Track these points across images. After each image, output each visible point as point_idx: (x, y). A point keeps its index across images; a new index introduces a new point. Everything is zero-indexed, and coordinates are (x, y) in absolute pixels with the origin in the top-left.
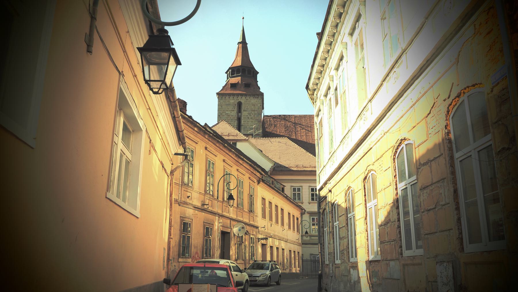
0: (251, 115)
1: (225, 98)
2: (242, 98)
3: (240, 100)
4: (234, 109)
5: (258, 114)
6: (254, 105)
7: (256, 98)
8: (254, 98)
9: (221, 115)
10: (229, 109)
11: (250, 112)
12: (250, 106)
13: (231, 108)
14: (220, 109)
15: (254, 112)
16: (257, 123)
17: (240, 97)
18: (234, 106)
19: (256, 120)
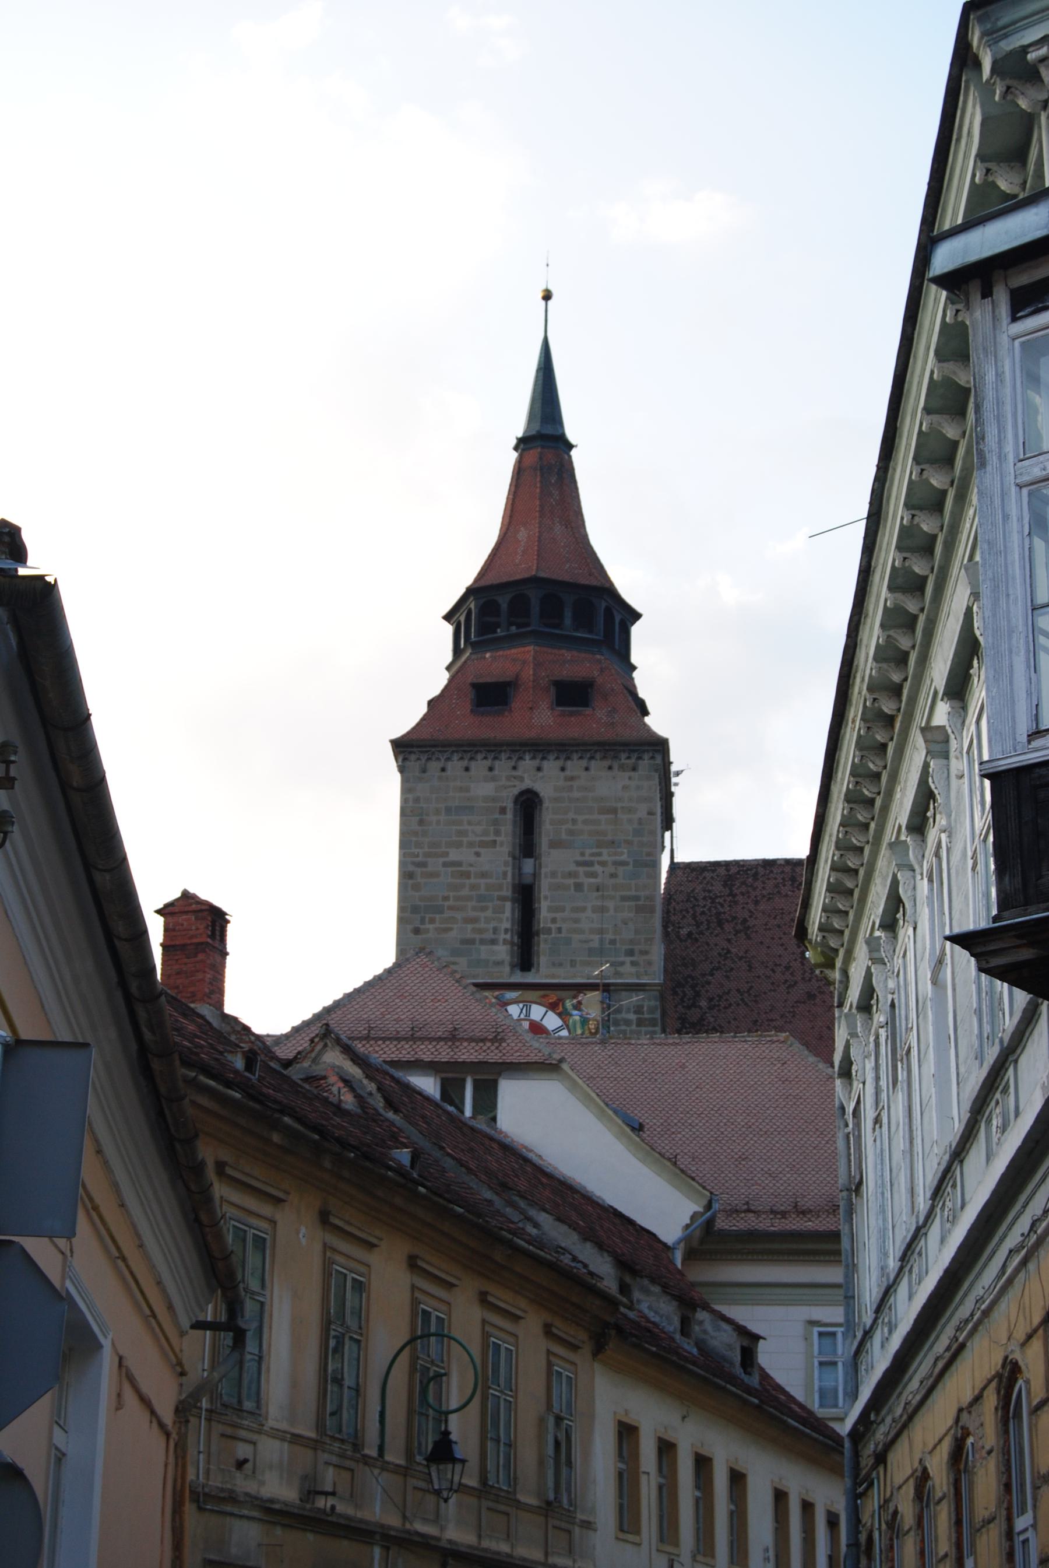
0: (597, 868)
1: (443, 770)
2: (539, 769)
3: (527, 784)
4: (497, 833)
5: (637, 864)
6: (614, 811)
7: (622, 768)
8: (610, 768)
9: (419, 870)
10: (462, 833)
11: (588, 852)
12: (587, 817)
13: (479, 829)
14: (416, 834)
15: (616, 854)
16: (632, 915)
17: (528, 763)
18: (497, 816)
19: (624, 899)
